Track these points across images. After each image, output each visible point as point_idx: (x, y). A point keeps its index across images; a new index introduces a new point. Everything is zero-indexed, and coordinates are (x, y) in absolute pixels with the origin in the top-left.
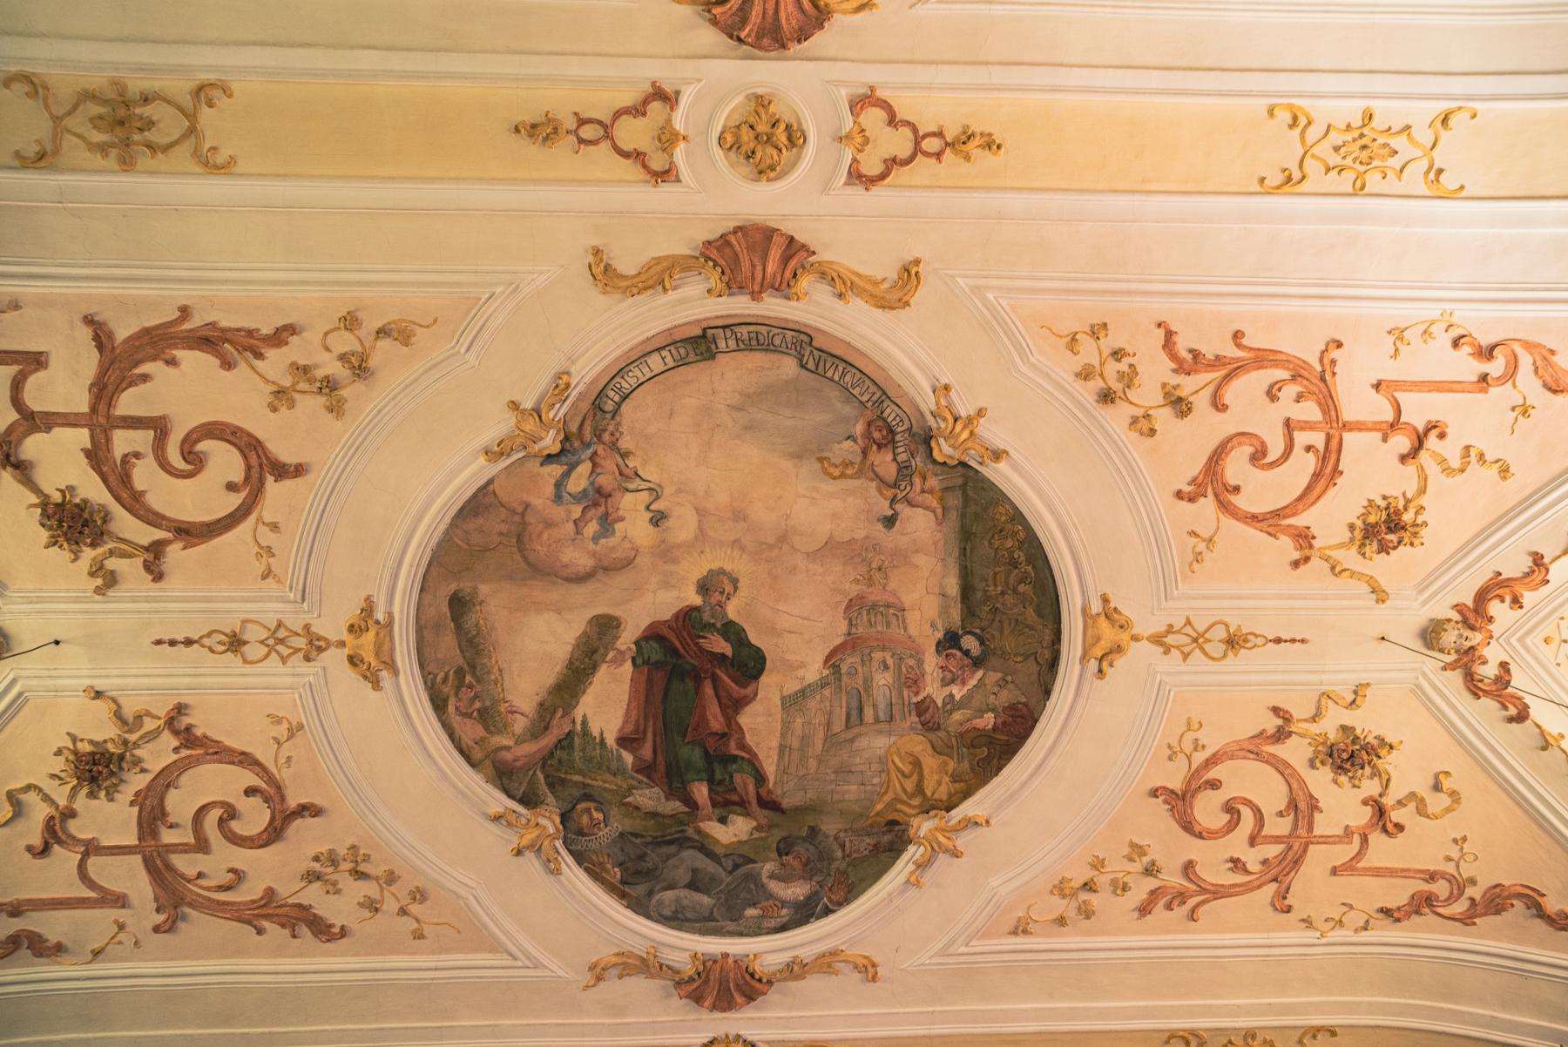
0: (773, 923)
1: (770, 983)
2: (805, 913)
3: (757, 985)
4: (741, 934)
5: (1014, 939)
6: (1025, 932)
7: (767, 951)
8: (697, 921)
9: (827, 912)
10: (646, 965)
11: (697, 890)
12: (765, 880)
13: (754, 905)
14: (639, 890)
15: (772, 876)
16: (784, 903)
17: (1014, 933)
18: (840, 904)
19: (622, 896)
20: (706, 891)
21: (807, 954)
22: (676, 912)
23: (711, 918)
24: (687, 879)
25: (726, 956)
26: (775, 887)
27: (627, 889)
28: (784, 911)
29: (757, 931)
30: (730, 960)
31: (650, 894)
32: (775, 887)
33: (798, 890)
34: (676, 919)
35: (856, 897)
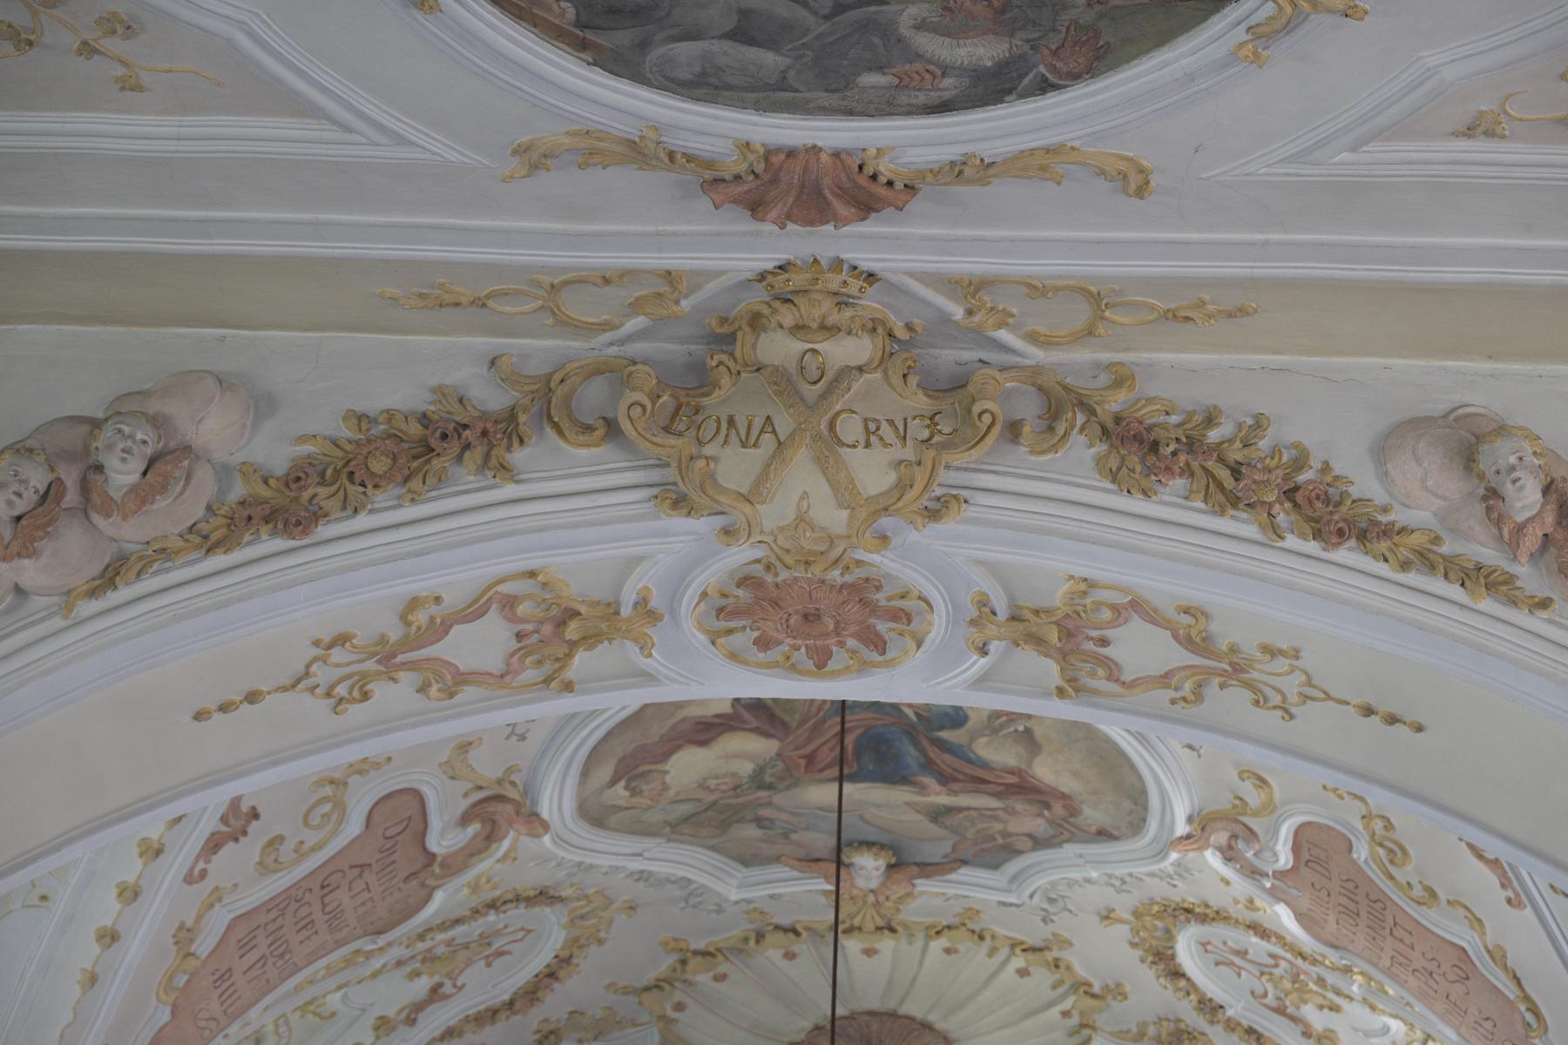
0: (922, 98)
1: (910, 188)
2: (991, 87)
3: (883, 192)
4: (850, 113)
5: (1463, 144)
6: (1489, 134)
7: (905, 141)
8: (752, 89)
9: (1045, 87)
10: (637, 152)
11: (752, 42)
12: (905, 30)
13: (881, 69)
14: (622, 38)
15: (921, 26)
16: (946, 70)
17: (1469, 132)
18: (1075, 77)
19: (581, 46)
20: (772, 44)
21: (993, 149)
22: (704, 74)
23: (782, 85)
24: (730, 24)
25: (815, 150)
26: (927, 43)
27: (590, 35)
28: (948, 82)
29: (885, 108)
30: (824, 157)
31: (644, 45)
32: (927, 43)
33: (981, 50)
34: (704, 85)
35: (1114, 66)
